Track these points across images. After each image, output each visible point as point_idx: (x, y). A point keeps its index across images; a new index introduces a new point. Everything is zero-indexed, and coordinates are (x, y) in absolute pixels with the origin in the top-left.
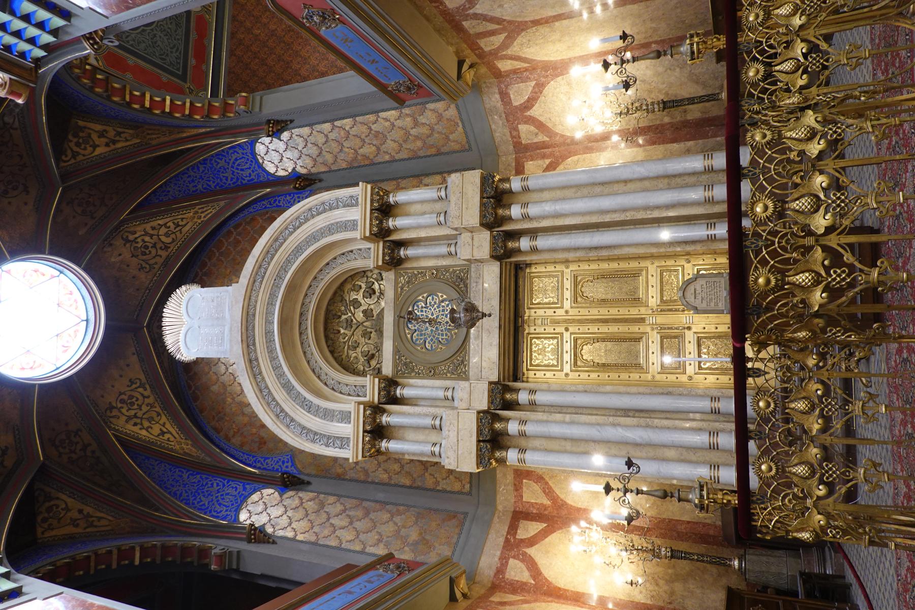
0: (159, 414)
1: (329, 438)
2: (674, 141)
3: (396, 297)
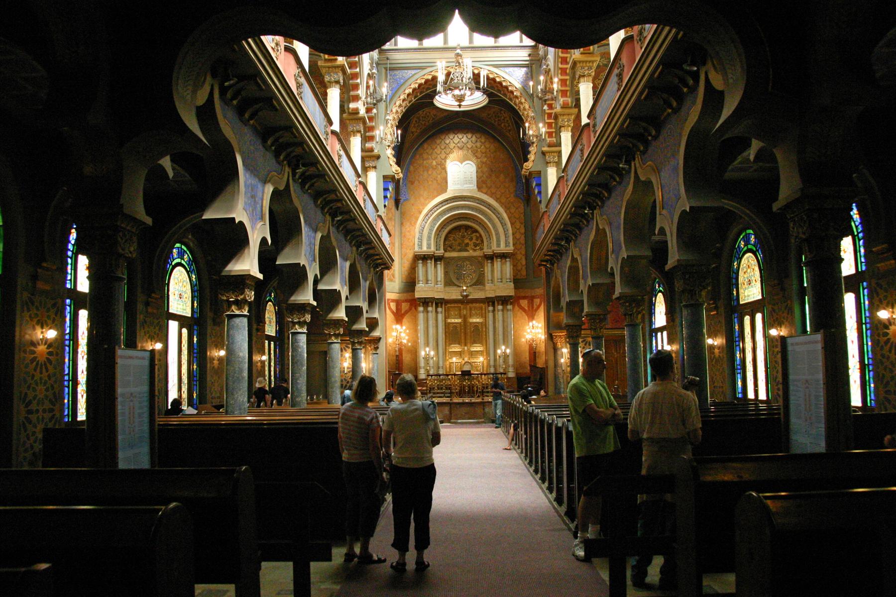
3: (473, 257)
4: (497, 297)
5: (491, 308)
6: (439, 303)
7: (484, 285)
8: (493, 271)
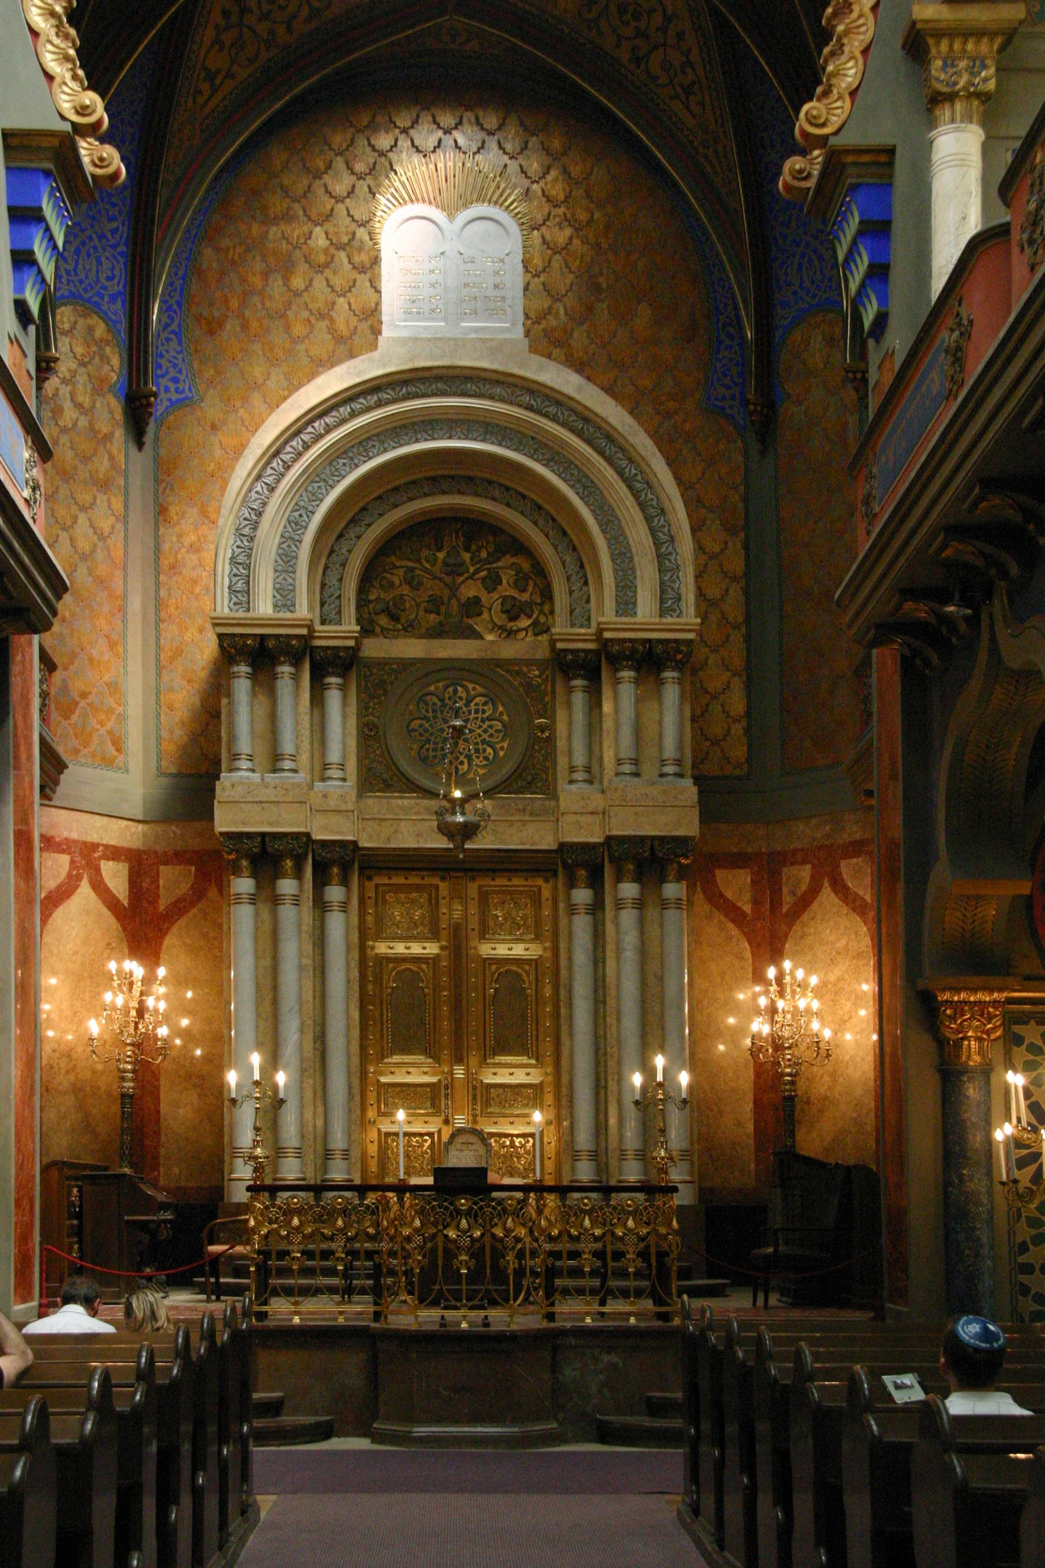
0: (251, 61)
3: (499, 663)
4: (609, 839)
5: (582, 895)
6: (333, 862)
7: (552, 794)
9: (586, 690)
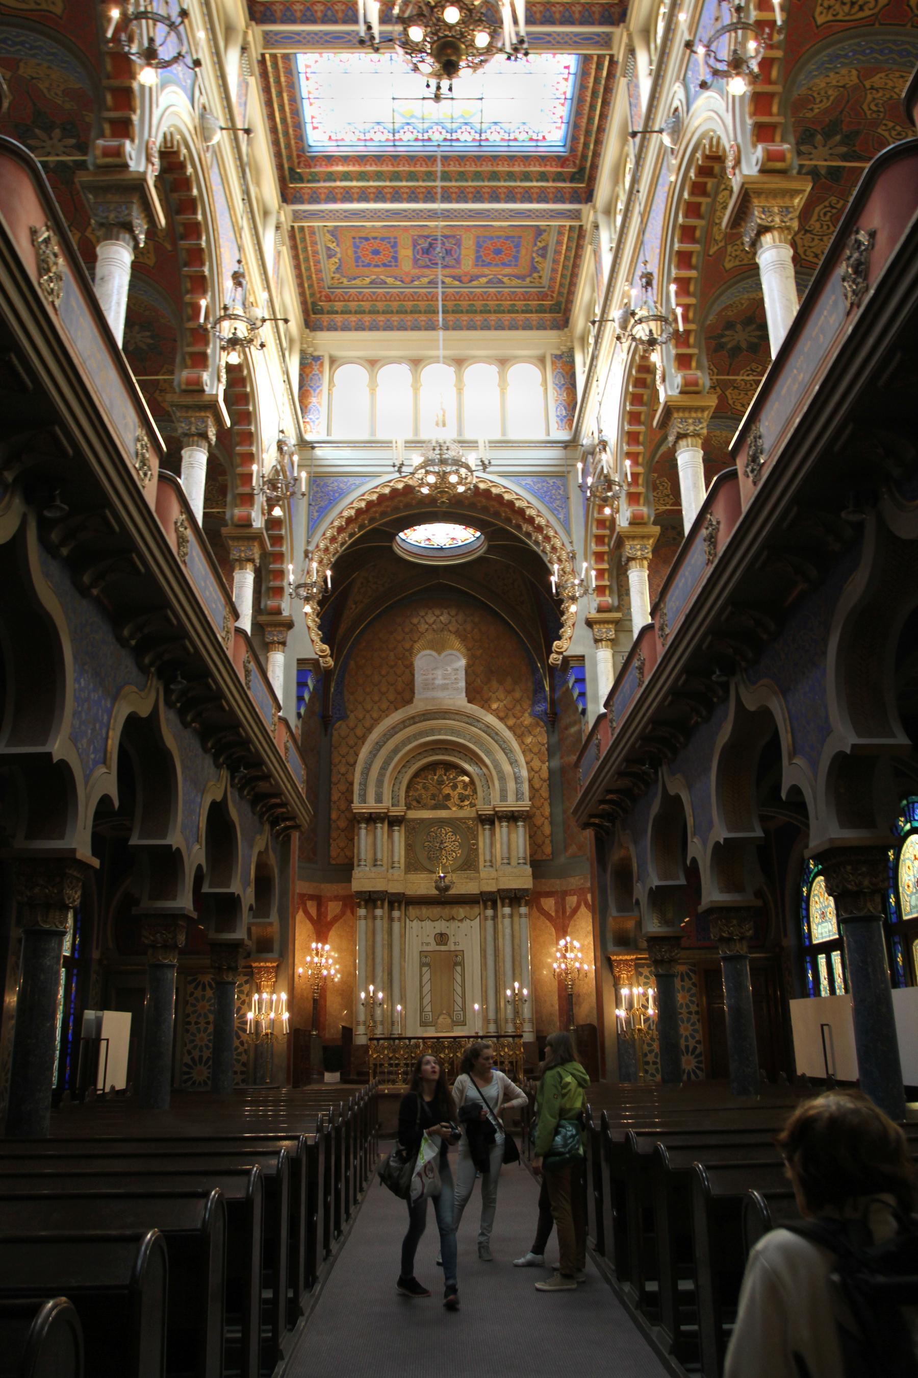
1: (365, 785)
2: (560, 997)
4: (499, 890)
5: (490, 912)
7: (477, 871)
8: (492, 844)
9: (490, 829)
